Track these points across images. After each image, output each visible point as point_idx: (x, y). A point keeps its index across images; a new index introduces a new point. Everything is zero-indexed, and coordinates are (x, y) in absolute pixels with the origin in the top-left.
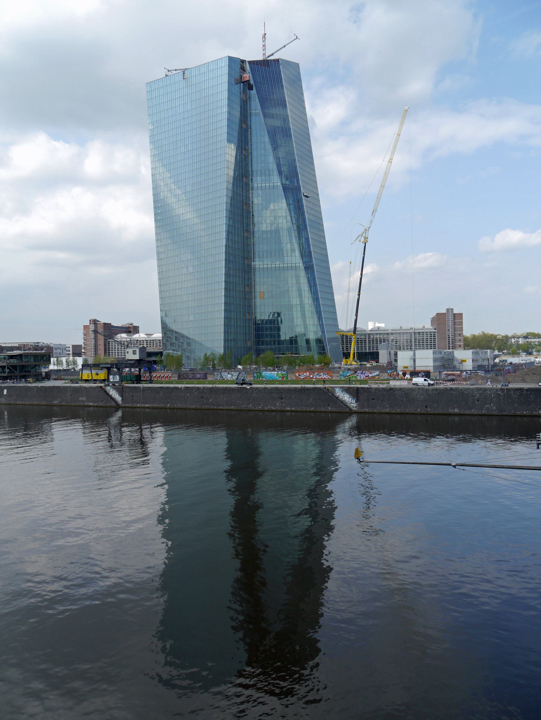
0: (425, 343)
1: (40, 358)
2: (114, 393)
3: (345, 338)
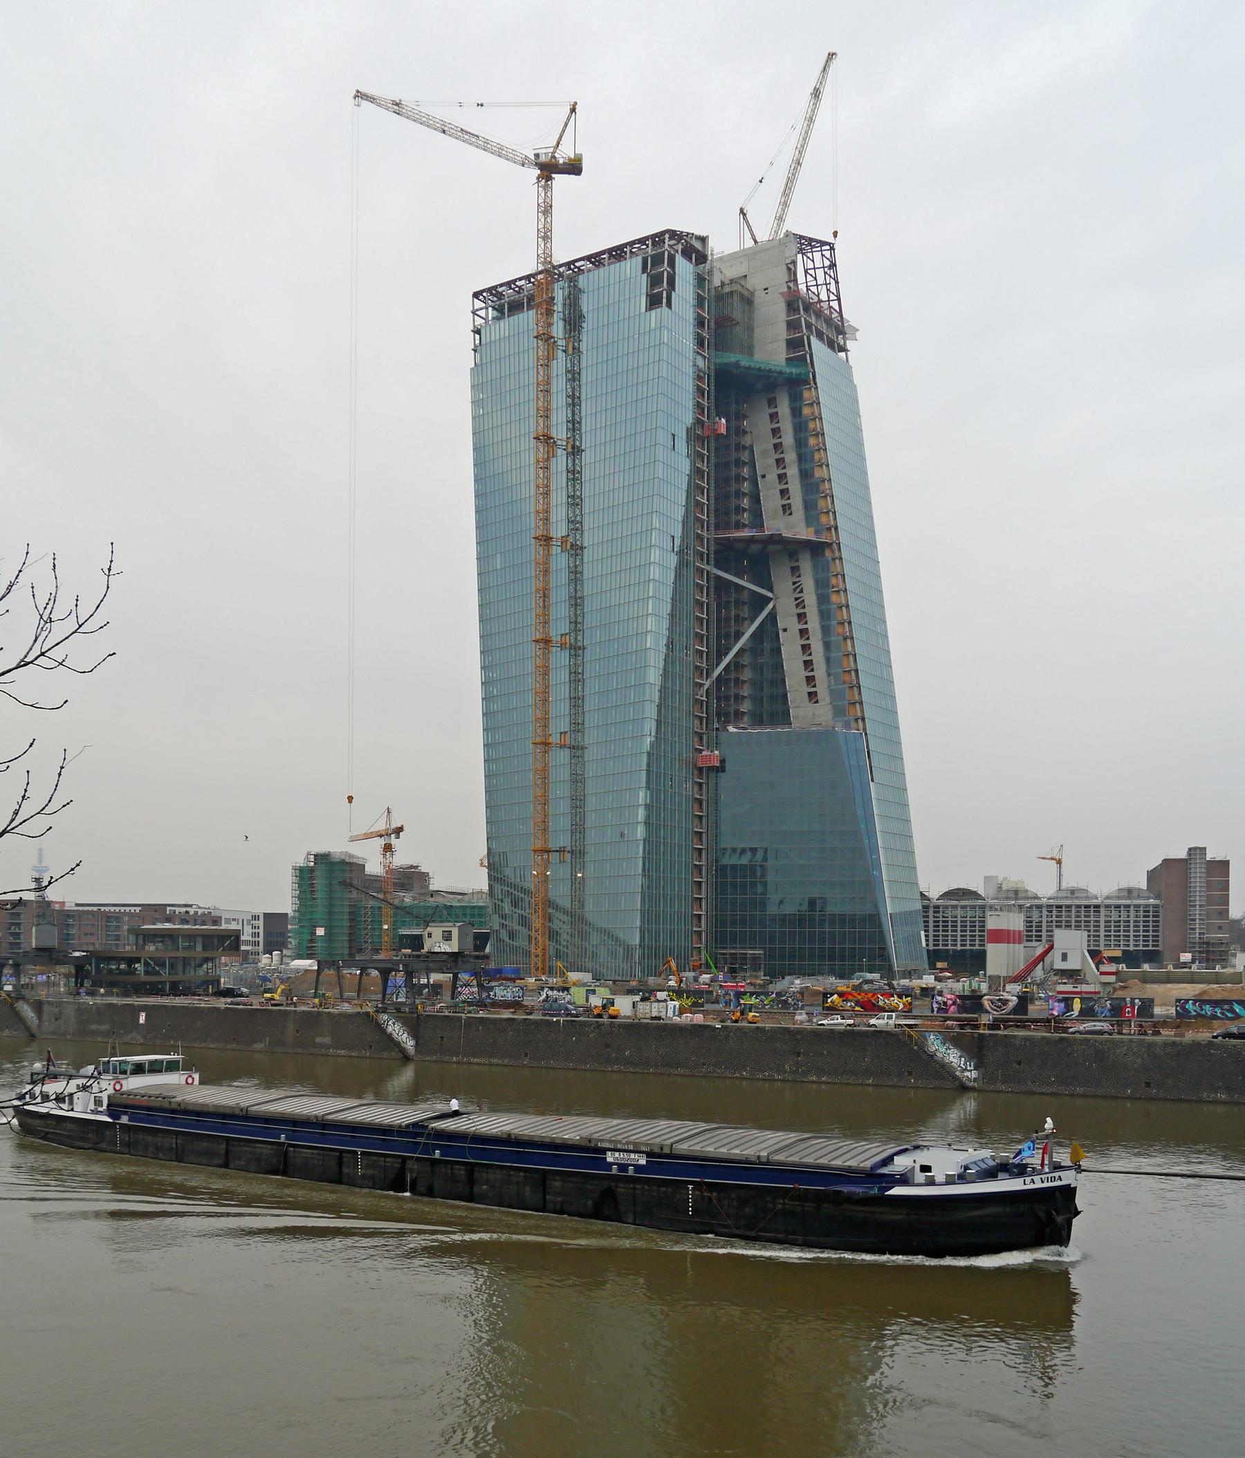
0: (1131, 931)
1: (215, 941)
2: (396, 1030)
3: (931, 914)
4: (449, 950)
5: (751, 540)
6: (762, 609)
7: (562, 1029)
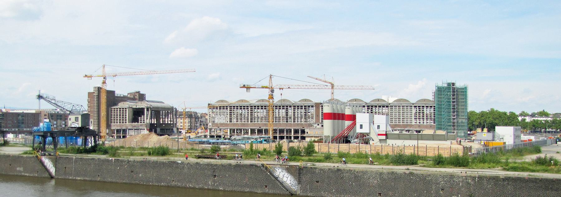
4: (77, 126)
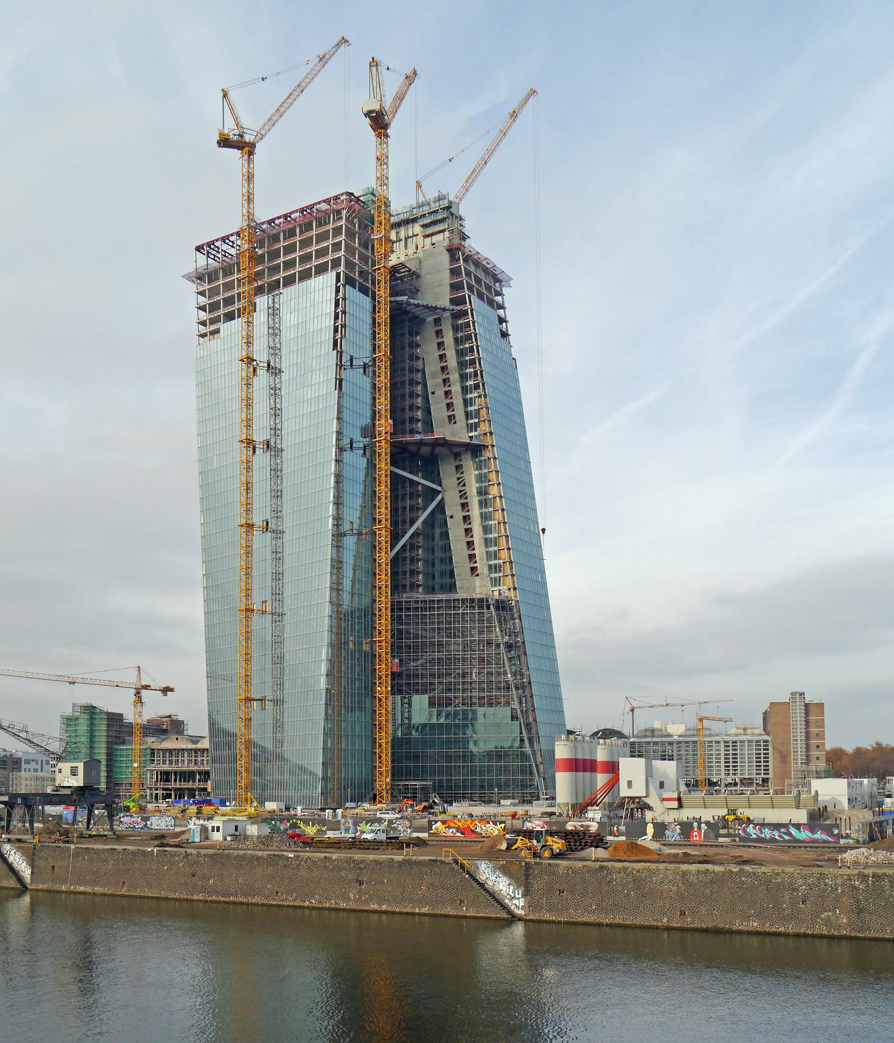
4: (76, 784)
5: (421, 443)
6: (433, 500)
7: (155, 859)
